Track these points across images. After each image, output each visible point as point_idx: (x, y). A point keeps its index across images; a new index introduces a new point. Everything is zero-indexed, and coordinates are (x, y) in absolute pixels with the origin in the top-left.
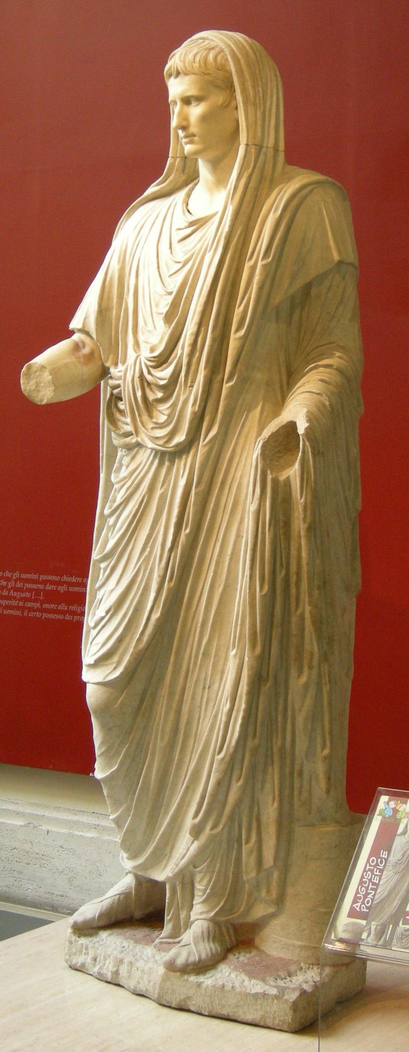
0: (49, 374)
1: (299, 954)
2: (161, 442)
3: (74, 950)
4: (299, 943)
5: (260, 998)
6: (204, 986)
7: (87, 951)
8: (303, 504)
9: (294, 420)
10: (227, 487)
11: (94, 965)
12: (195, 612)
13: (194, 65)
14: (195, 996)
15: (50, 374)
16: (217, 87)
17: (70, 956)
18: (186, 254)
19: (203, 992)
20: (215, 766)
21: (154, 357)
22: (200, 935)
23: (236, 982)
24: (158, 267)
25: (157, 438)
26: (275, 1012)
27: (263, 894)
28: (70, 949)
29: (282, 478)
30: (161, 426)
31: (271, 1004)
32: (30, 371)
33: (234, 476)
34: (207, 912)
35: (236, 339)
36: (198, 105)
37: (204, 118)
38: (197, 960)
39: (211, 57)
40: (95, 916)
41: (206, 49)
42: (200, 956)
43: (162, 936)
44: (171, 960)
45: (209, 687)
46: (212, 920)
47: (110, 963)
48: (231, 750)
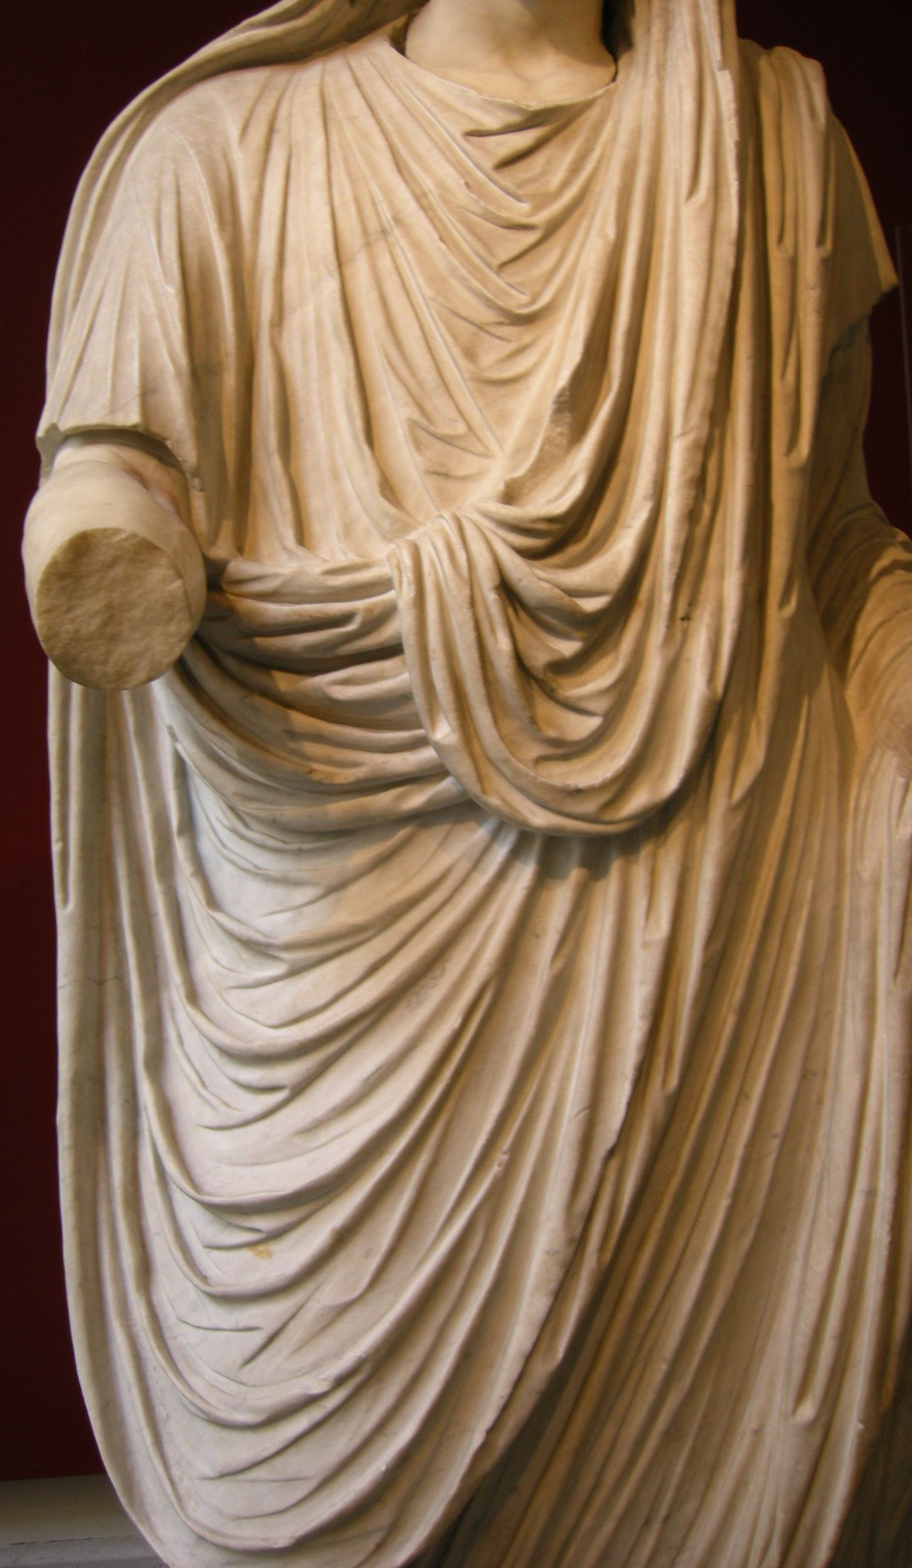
0: (171, 572)
2: (590, 806)
15: (179, 575)
18: (538, 208)
21: (551, 520)
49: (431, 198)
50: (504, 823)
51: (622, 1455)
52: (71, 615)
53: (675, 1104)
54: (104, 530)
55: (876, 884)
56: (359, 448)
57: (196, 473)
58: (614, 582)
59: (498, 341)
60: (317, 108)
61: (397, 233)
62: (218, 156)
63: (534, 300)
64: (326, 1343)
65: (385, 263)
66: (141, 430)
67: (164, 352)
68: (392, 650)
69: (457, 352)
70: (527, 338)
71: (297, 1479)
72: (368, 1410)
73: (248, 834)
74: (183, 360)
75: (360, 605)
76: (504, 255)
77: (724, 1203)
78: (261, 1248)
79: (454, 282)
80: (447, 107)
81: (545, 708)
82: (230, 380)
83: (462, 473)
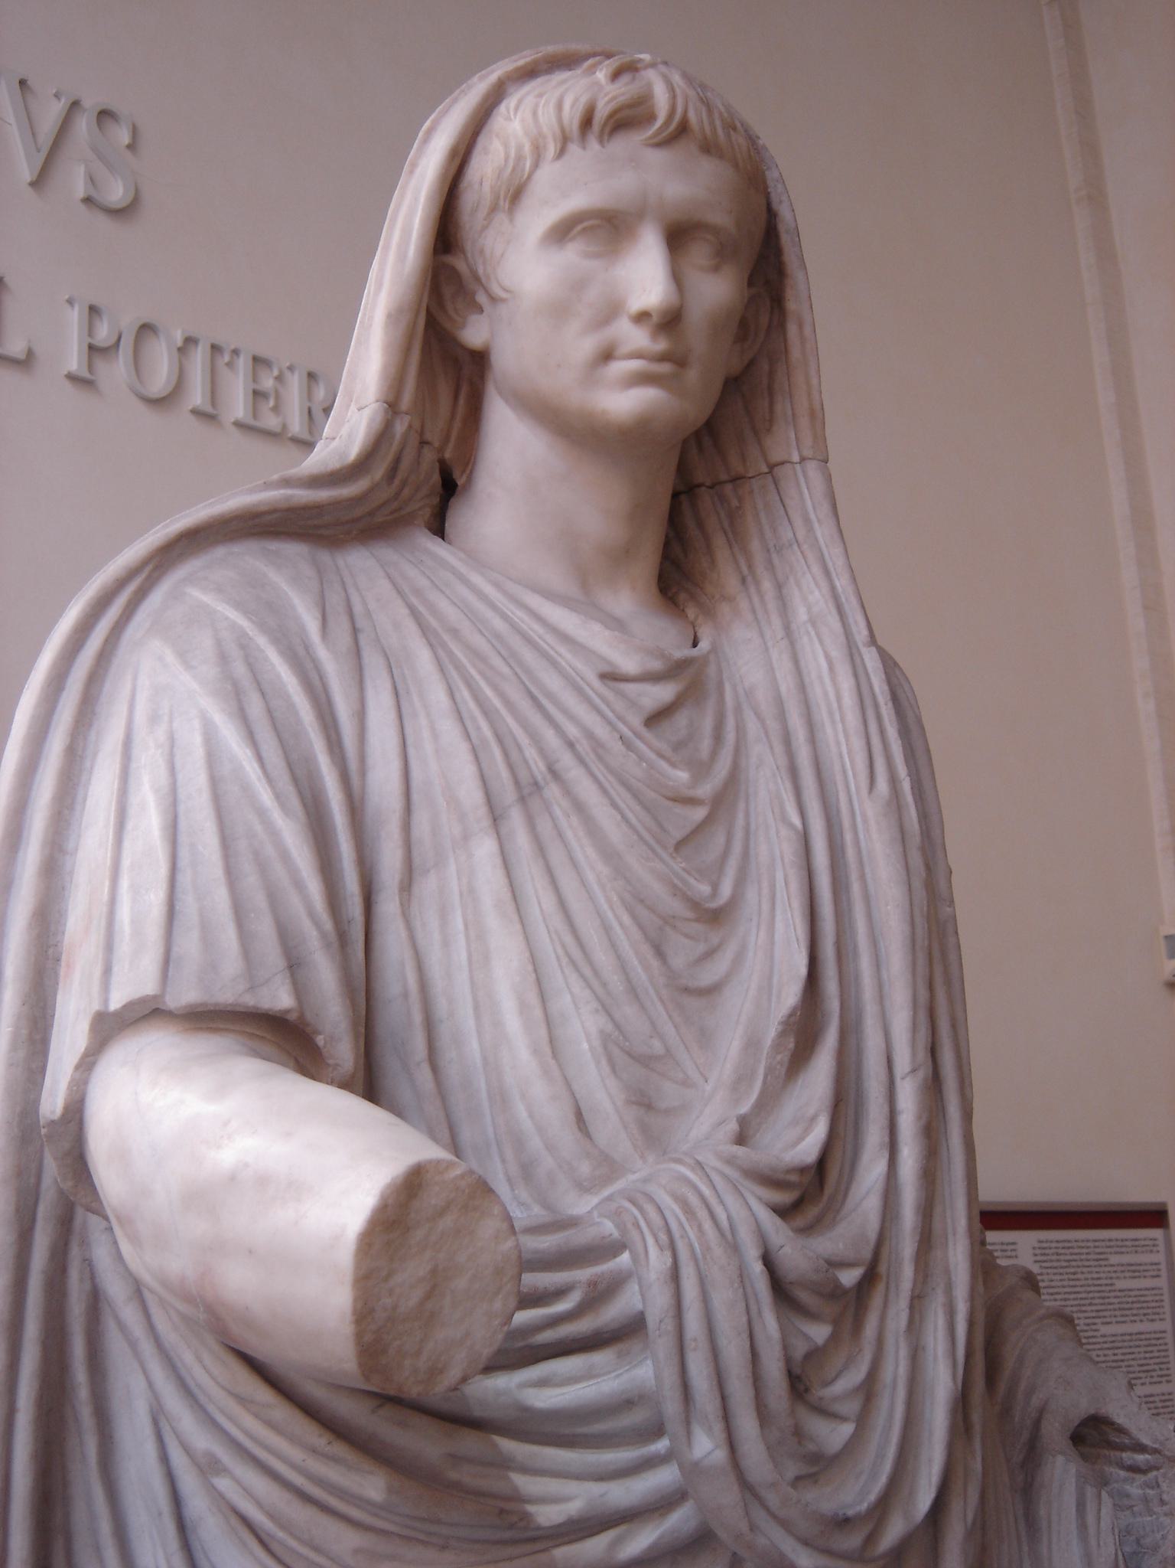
61: (553, 791)
66: (293, 1017)
70: (715, 940)
75: (583, 1275)
76: (678, 835)
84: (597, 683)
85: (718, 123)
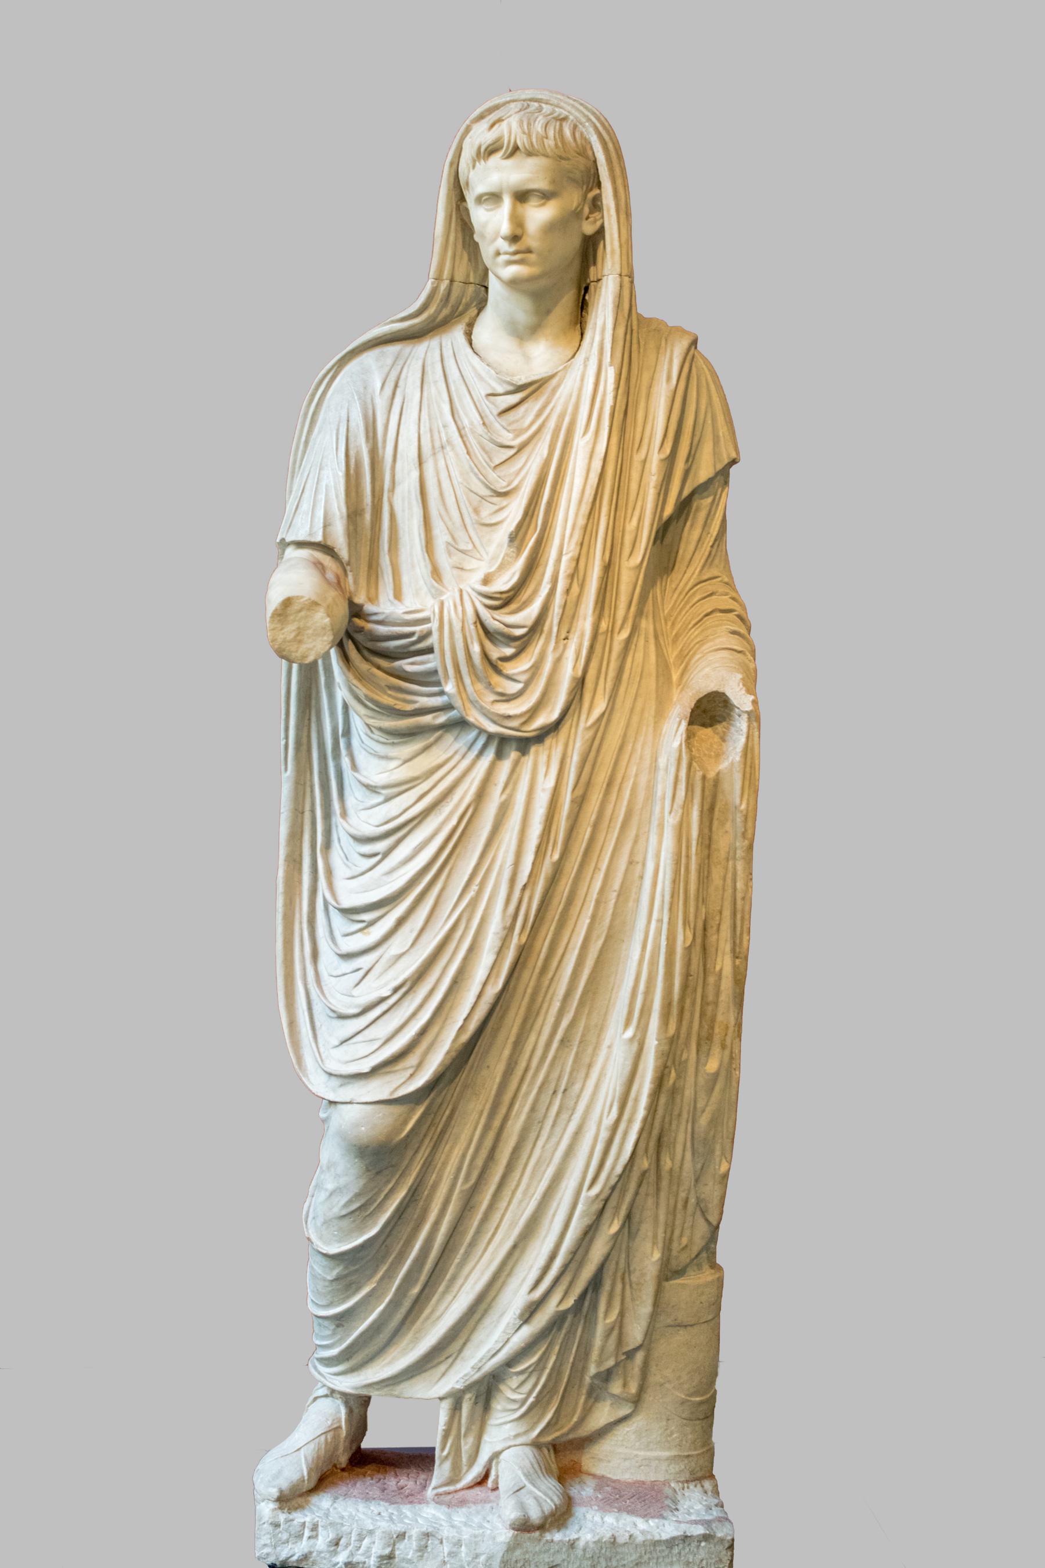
0: (325, 615)
1: (667, 1471)
2: (515, 723)
3: (285, 1536)
4: (667, 1454)
5: (677, 1545)
6: (581, 1544)
7: (314, 1533)
8: (744, 812)
9: (721, 690)
10: (615, 789)
11: (335, 1553)
12: (552, 979)
13: (546, 144)
14: (566, 1564)
15: (328, 616)
16: (573, 180)
17: (275, 1548)
18: (517, 436)
19: (580, 1552)
20: (580, 1207)
21: (501, 593)
22: (532, 1471)
23: (628, 1529)
24: (468, 453)
25: (509, 717)
26: (702, 1561)
27: (616, 1387)
28: (275, 1536)
29: (711, 775)
30: (508, 698)
31: (695, 1550)
32: (289, 609)
33: (625, 772)
34: (526, 1432)
35: (630, 569)
36: (543, 205)
37: (551, 228)
38: (554, 1507)
39: (567, 132)
40: (303, 1474)
41: (556, 119)
42: (552, 1500)
43: (434, 1482)
44: (524, 1516)
45: (565, 1090)
46: (536, 1444)
47: (374, 1543)
48: (613, 1180)
49: (466, 429)
50: (481, 731)
51: (539, 1053)
52: (283, 631)
53: (558, 869)
54: (298, 596)
55: (666, 770)
56: (423, 554)
57: (349, 564)
58: (530, 622)
59: (491, 505)
60: (419, 375)
62: (369, 401)
63: (508, 485)
64: (391, 973)
65: (441, 463)
66: (322, 543)
67: (336, 505)
68: (430, 650)
69: (470, 510)
71: (375, 1040)
72: (409, 1006)
73: (372, 735)
74: (344, 510)
75: (417, 629)
76: (497, 462)
77: (588, 921)
78: (365, 931)
79: (472, 475)
80: (481, 378)
81: (496, 679)
82: (368, 517)
83: (468, 568)
84: (484, 398)
85: (534, 140)
